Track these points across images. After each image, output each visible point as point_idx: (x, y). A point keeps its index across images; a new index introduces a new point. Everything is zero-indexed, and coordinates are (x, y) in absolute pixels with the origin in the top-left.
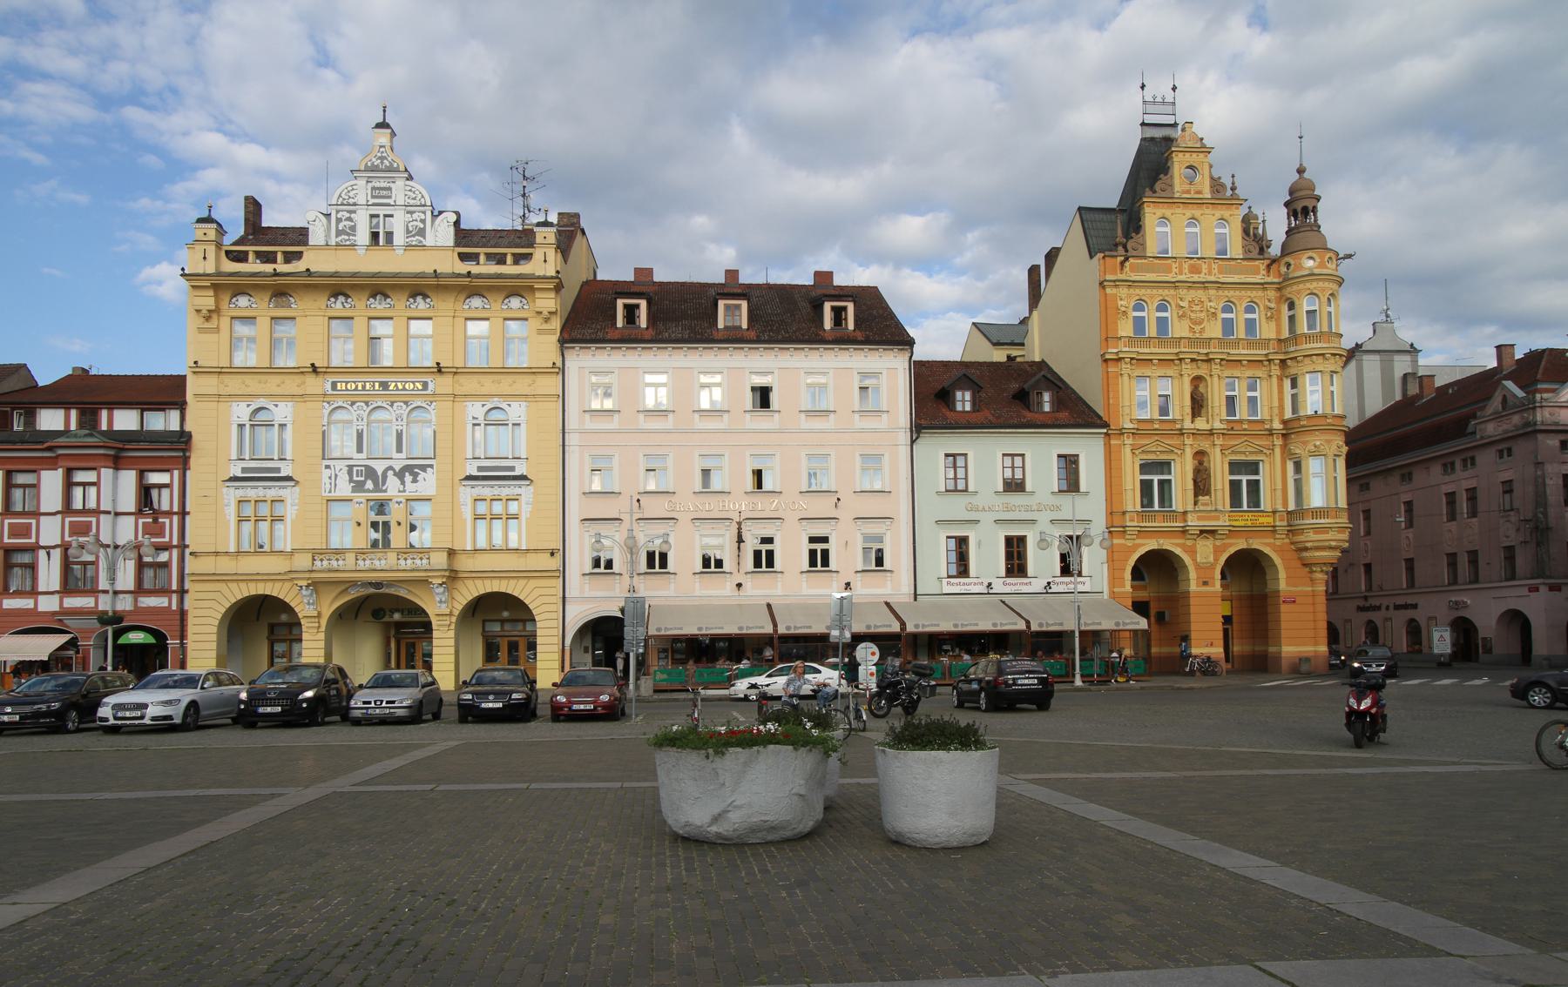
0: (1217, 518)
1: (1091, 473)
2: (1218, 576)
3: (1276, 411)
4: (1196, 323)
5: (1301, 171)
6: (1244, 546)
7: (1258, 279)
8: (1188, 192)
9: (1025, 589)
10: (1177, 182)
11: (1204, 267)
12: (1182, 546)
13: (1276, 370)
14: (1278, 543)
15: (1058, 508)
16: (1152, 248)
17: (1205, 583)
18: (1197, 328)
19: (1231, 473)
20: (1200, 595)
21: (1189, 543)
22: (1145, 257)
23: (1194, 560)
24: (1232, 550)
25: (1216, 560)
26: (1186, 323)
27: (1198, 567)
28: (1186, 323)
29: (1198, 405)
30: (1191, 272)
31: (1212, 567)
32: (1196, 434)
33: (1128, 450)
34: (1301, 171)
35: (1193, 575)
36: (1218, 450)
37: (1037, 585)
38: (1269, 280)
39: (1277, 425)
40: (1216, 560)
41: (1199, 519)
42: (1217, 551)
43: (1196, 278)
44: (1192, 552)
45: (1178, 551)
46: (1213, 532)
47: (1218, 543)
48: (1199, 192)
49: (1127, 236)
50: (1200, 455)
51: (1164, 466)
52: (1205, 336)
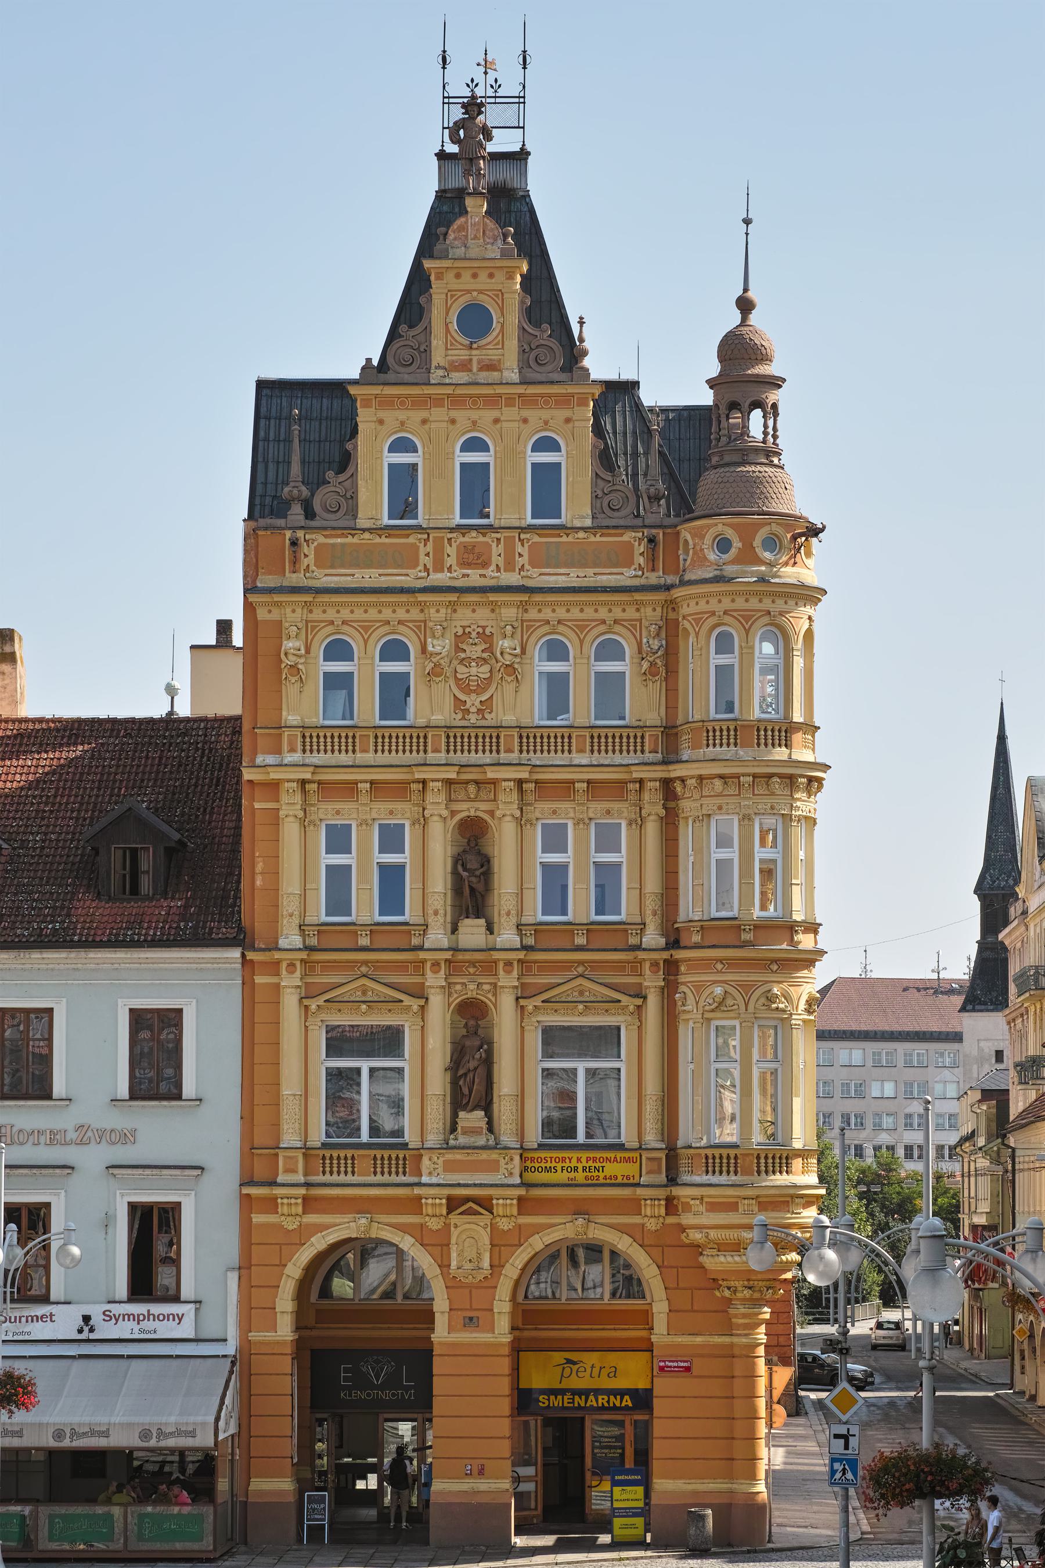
0: (492, 1167)
1: (209, 1056)
3: (651, 904)
4: (467, 689)
5: (745, 305)
7: (626, 576)
8: (464, 366)
9: (40, 1330)
10: (437, 343)
11: (497, 552)
13: (653, 805)
14: (652, 1225)
15: (126, 1137)
16: (375, 502)
17: (470, 1322)
18: (473, 701)
19: (548, 1055)
20: (457, 1351)
22: (353, 530)
23: (444, 1266)
25: (496, 1267)
26: (444, 692)
27: (453, 1285)
28: (444, 692)
29: (472, 889)
30: (464, 564)
32: (456, 962)
33: (290, 1003)
34: (745, 305)
37: (64, 1322)
38: (653, 578)
39: (652, 938)
40: (496, 1267)
41: (450, 1167)
42: (501, 1245)
43: (474, 577)
48: (491, 367)
49: (316, 482)
50: (472, 1016)
51: (389, 1041)
52: (491, 719)
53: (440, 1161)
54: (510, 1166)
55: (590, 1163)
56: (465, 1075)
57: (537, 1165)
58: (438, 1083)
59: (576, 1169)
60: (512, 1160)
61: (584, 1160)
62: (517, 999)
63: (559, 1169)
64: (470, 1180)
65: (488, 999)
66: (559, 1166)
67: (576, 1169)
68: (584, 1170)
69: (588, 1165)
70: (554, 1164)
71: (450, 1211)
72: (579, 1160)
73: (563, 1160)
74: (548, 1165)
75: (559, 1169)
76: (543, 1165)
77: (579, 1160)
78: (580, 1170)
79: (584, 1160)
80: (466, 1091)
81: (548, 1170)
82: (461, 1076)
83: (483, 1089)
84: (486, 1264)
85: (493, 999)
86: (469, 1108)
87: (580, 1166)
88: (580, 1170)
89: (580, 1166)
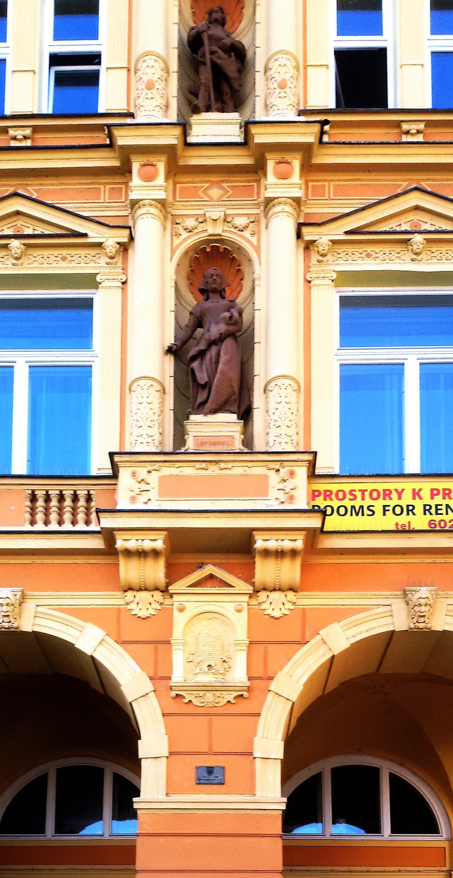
2: (270, 741)
6: (399, 620)
12: (117, 625)
17: (209, 777)
19: (350, 335)
21: (144, 604)
23: (160, 677)
24: (339, 638)
25: (260, 679)
27: (178, 707)
31: (246, 702)
35: (153, 742)
36: (283, 224)
42: (267, 645)
44: (154, 645)
45: (88, 639)
46: (236, 548)
47: (276, 605)
50: (214, 271)
53: (153, 478)
54: (288, 486)
55: (438, 499)
56: (201, 354)
57: (336, 504)
58: (153, 364)
59: (410, 510)
60: (292, 474)
61: (425, 494)
62: (300, 226)
63: (378, 509)
64: (211, 506)
65: (245, 240)
66: (378, 506)
67: (410, 510)
68: (426, 509)
69: (433, 503)
70: (367, 502)
71: (174, 573)
72: (416, 494)
73: (387, 494)
74: (357, 503)
75: (378, 509)
76: (348, 503)
77: (416, 494)
78: (419, 510)
79: (425, 494)
80: (202, 377)
81: (358, 511)
82: (194, 358)
83: (235, 375)
84: (239, 675)
85: (254, 240)
86: (209, 405)
87: (419, 505)
88: (419, 510)
89: (419, 505)
